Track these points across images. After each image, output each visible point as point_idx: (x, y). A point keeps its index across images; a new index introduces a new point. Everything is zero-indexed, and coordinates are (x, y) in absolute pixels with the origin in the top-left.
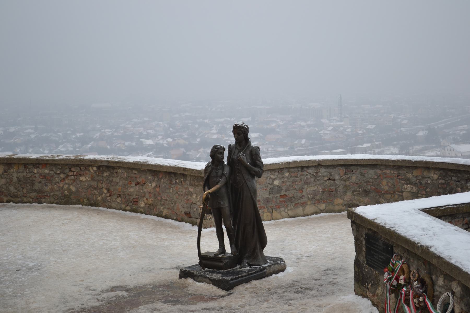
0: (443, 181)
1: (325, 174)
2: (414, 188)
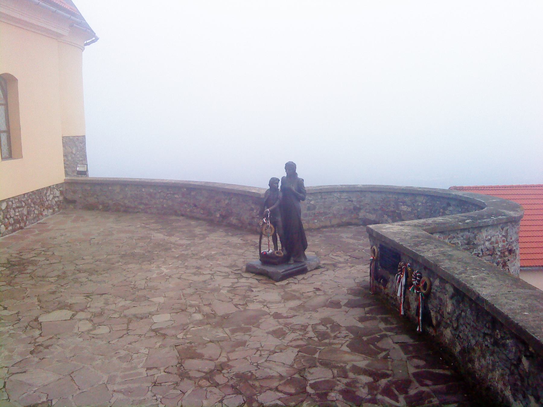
1: (346, 197)
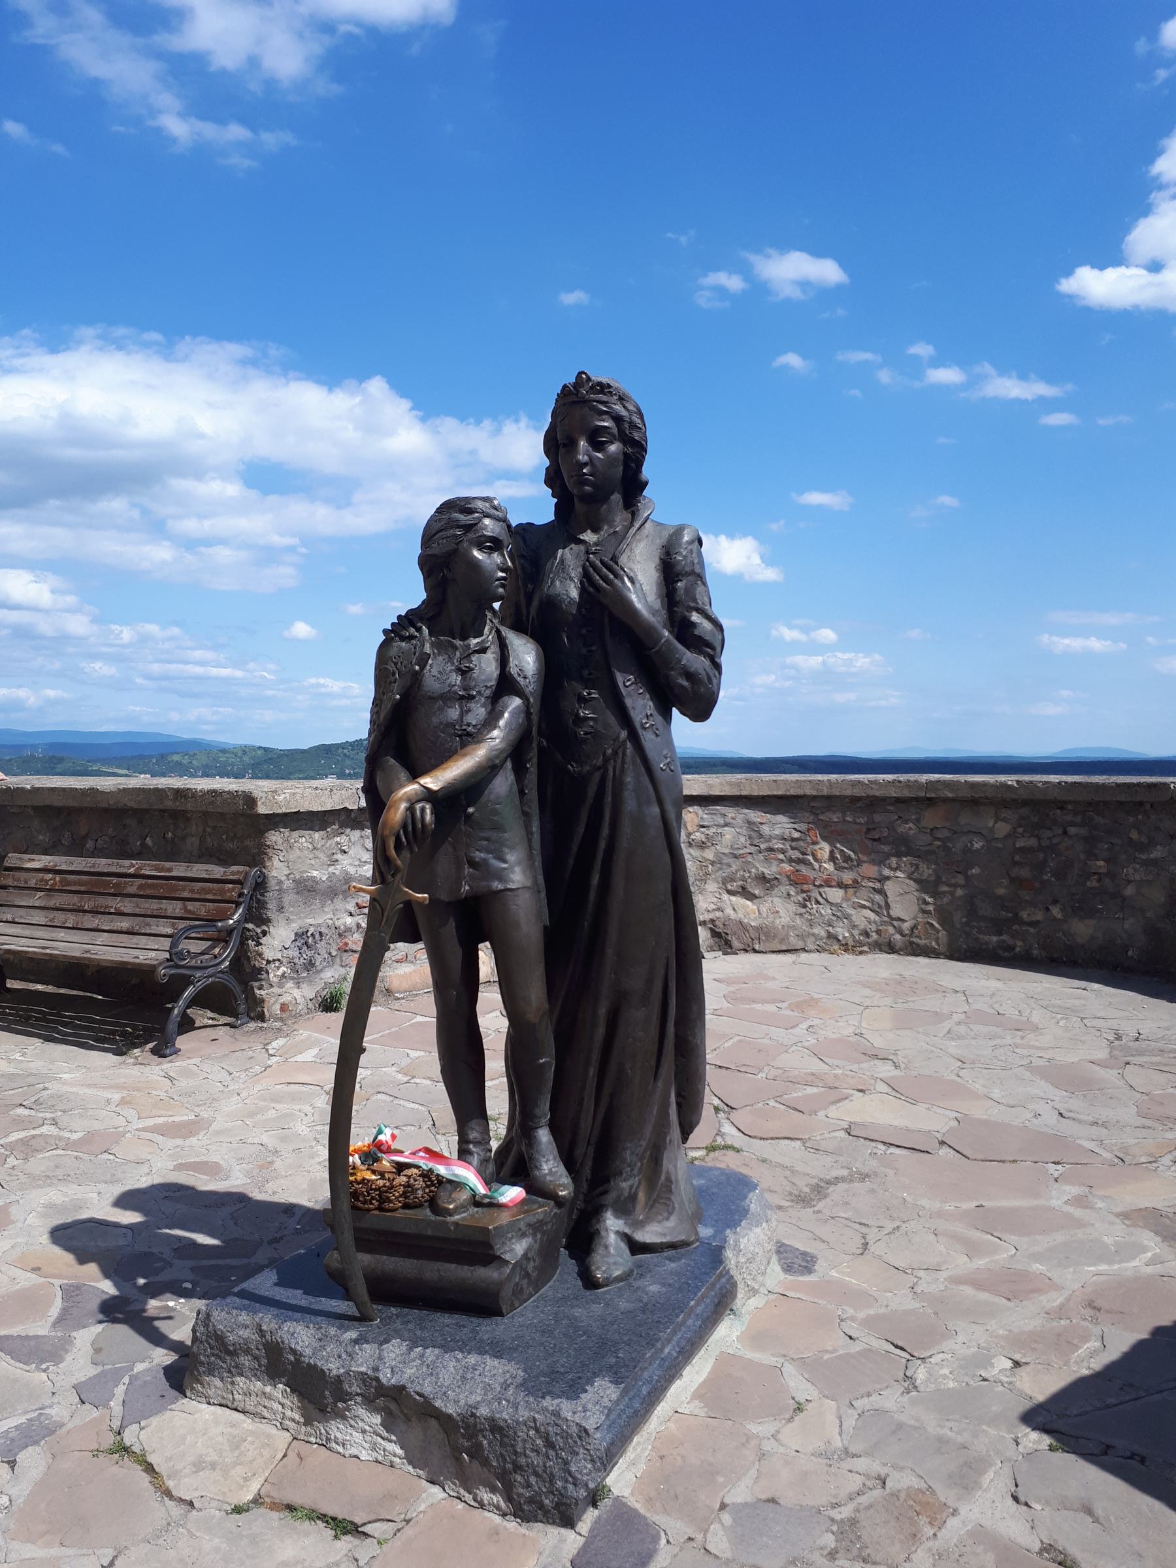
0: (1033, 842)
2: (923, 866)
